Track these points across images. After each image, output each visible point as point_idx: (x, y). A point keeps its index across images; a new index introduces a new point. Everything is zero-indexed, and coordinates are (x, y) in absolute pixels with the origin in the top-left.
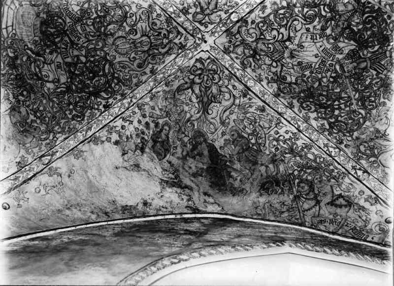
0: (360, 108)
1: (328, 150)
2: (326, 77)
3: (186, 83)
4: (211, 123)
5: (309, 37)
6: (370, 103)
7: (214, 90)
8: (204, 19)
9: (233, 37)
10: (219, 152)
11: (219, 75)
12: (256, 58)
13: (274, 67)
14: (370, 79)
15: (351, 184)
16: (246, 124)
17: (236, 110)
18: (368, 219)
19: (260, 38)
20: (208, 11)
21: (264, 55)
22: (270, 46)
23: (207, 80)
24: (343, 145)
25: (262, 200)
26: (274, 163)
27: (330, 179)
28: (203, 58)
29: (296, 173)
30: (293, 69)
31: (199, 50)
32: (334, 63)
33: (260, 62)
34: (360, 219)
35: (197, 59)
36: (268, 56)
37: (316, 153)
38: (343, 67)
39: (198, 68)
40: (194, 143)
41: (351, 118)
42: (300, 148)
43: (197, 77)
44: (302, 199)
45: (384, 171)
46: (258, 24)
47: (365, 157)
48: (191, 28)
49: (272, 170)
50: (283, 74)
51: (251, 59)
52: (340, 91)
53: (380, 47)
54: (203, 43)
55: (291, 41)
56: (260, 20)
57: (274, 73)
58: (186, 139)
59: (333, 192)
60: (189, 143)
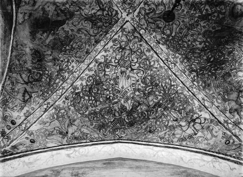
0: (89, 112)
1: (60, 89)
2: (110, 94)
3: (103, 6)
4: (79, 23)
5: (134, 82)
6: (92, 118)
7: (100, 24)
8: (142, 14)
9: (131, 34)
10: (60, 27)
11: (109, 26)
12: (120, 50)
13: (115, 61)
14: (108, 118)
15: (39, 103)
17: (87, 37)
18: (14, 110)
19: (132, 51)
20: (147, 18)
21: (122, 55)
22: (128, 58)
23: (105, 19)
24: (65, 100)
25: (28, 50)
26: (53, 59)
27: (42, 91)
28: (118, 15)
29: (47, 72)
30: (115, 73)
31: (122, 11)
32: (118, 98)
33: (117, 52)
34: (14, 106)
35: (117, 11)
36: (121, 57)
37: (60, 84)
38: (116, 104)
39: (113, 13)
40: (66, 11)
41: (83, 106)
42: (63, 75)
43: (107, 13)
44: (29, 74)
45: (48, 122)
46: (140, 49)
47: (57, 112)
48: (135, 5)
49: (49, 58)
50: (111, 66)
51: (119, 46)
52: (101, 102)
53: (127, 122)
54: (126, 14)
55: (131, 70)
56: (142, 49)
57: (111, 60)
58: (67, 6)
59: (34, 92)
60: (65, 8)
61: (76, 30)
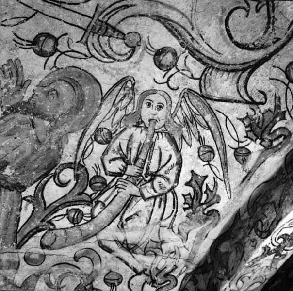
16: (123, 139)
61: (76, 34)
